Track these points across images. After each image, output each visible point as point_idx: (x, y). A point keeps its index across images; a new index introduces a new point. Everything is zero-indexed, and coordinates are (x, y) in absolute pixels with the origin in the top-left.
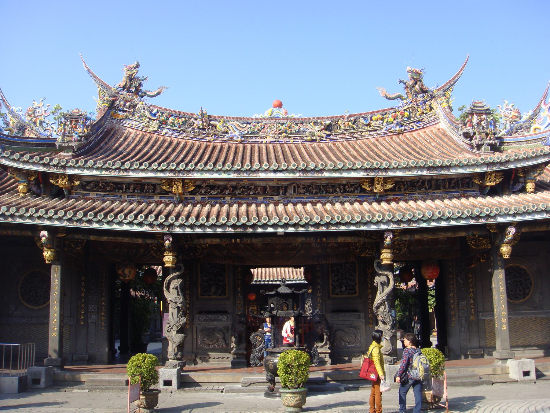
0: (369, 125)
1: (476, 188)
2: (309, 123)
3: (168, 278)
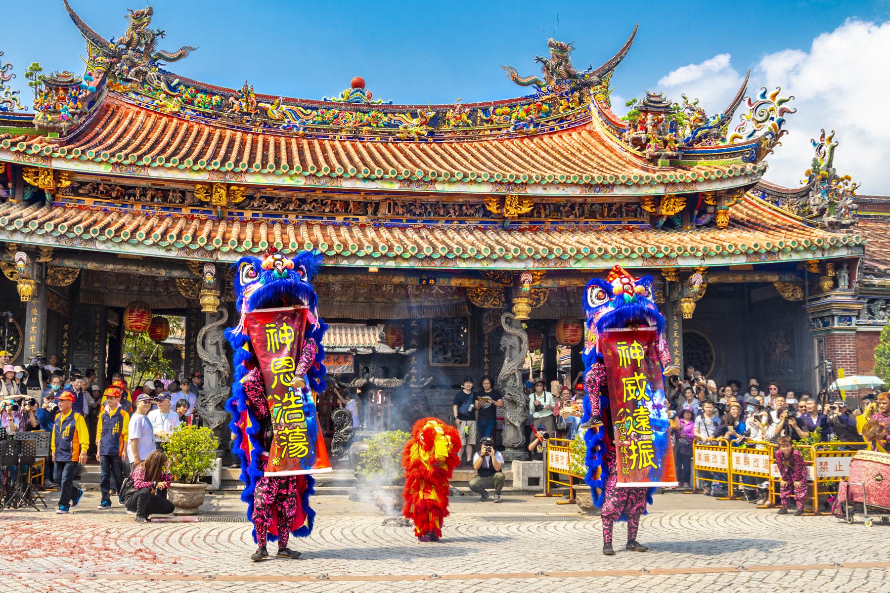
1: (646, 218)
3: (204, 329)
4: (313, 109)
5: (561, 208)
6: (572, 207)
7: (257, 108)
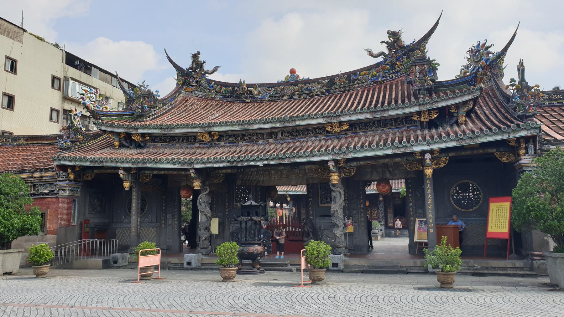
0: (358, 79)
2: (315, 83)
4: (272, 88)
5: (368, 124)
6: (374, 123)
7: (248, 90)
